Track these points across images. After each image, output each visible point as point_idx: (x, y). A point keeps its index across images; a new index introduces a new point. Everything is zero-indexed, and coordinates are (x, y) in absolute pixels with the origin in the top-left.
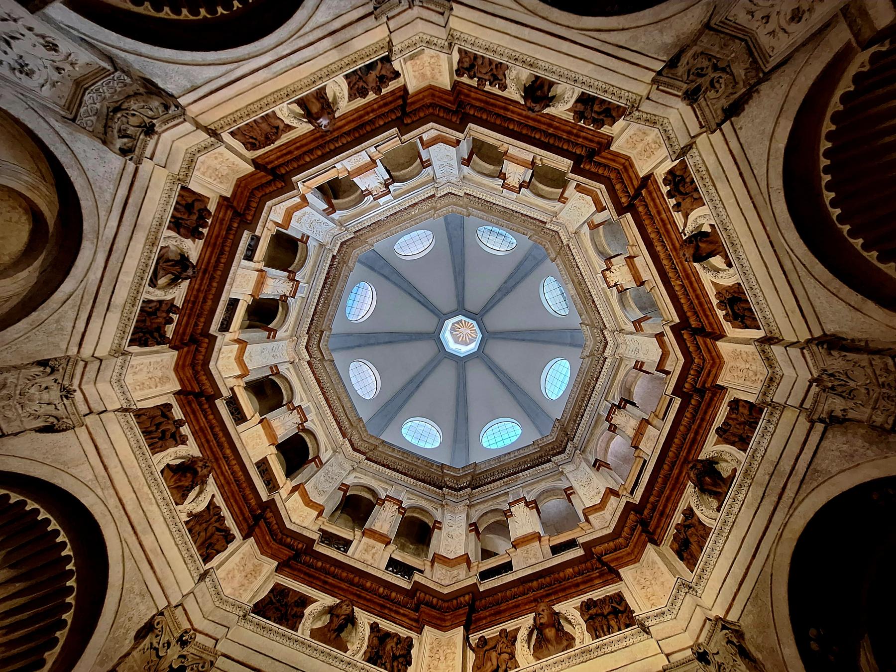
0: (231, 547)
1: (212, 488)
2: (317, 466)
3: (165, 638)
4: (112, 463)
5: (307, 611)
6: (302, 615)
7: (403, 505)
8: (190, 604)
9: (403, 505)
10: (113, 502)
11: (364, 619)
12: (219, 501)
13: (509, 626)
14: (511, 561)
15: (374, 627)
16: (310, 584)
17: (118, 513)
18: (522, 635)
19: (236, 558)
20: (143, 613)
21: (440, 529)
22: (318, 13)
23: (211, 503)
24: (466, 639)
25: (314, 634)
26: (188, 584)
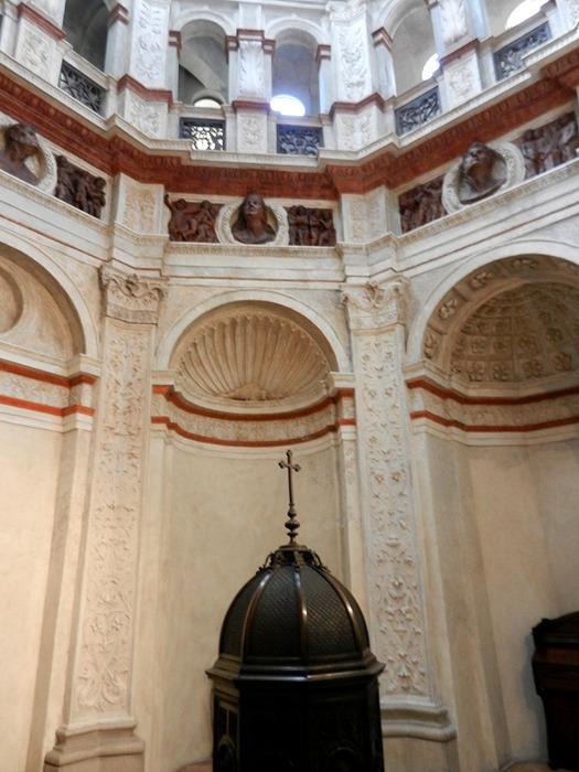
21: (328, 58)
23: (60, 161)
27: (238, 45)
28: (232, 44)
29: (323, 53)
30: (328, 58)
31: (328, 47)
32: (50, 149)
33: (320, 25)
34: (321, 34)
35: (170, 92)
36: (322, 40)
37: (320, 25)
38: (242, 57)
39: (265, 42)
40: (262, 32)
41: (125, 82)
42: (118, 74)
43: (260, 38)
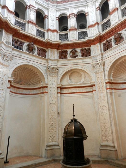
1: (36, 46)
7: (75, 14)
9: (75, 14)
11: (79, 50)
12: (38, 47)
13: (110, 38)
14: (110, 19)
18: (112, 40)
21: (88, 15)
22: (20, 62)
23: (37, 47)
27: (70, 17)
28: (68, 17)
29: (87, 14)
30: (88, 15)
31: (88, 13)
32: (36, 46)
33: (86, 8)
34: (86, 10)
35: (57, 30)
36: (86, 12)
37: (86, 8)
38: (70, 20)
39: (75, 15)
40: (74, 14)
41: (49, 30)
42: (47, 29)
43: (74, 15)
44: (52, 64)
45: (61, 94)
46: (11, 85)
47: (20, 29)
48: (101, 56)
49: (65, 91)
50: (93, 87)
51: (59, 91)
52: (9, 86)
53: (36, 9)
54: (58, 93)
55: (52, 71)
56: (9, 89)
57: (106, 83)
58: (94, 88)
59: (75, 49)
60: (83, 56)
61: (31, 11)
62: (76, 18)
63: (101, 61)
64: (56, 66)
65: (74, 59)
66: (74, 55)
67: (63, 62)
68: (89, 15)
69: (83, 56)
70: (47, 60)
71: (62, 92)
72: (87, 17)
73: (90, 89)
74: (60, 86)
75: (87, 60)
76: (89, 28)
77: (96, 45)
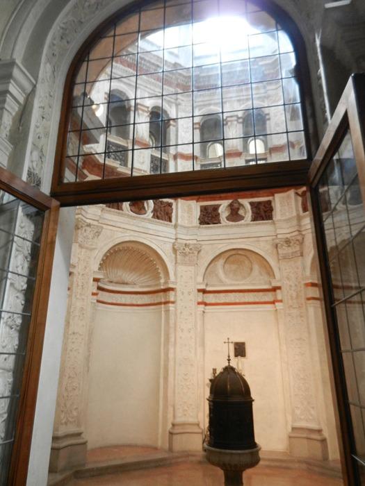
0: (174, 207)
2: (174, 126)
3: (182, 248)
4: (118, 225)
5: (220, 210)
6: (219, 214)
8: (179, 236)
10: (132, 233)
11: (246, 202)
15: (251, 204)
16: (215, 200)
17: (136, 234)
19: (180, 211)
20: (169, 247)
24: (297, 193)
25: (228, 219)
26: (173, 231)
29: (267, 117)
31: (268, 114)
44: (185, 237)
45: (206, 304)
46: (99, 288)
47: (118, 166)
48: (295, 222)
49: (210, 298)
50: (278, 291)
51: (200, 300)
52: (95, 291)
53: (150, 109)
54: (199, 303)
55: (184, 252)
56: (95, 297)
57: (307, 285)
58: (279, 295)
59: (240, 200)
60: (254, 219)
61: (141, 117)
62: (241, 125)
63: (297, 233)
64: (195, 242)
65: (235, 226)
66: (235, 215)
67: (210, 231)
68: (271, 120)
69: (254, 219)
70: (176, 226)
71: (208, 301)
72: (268, 122)
73: (269, 297)
74: (203, 287)
75: (263, 228)
76: (270, 153)
77: (288, 193)
